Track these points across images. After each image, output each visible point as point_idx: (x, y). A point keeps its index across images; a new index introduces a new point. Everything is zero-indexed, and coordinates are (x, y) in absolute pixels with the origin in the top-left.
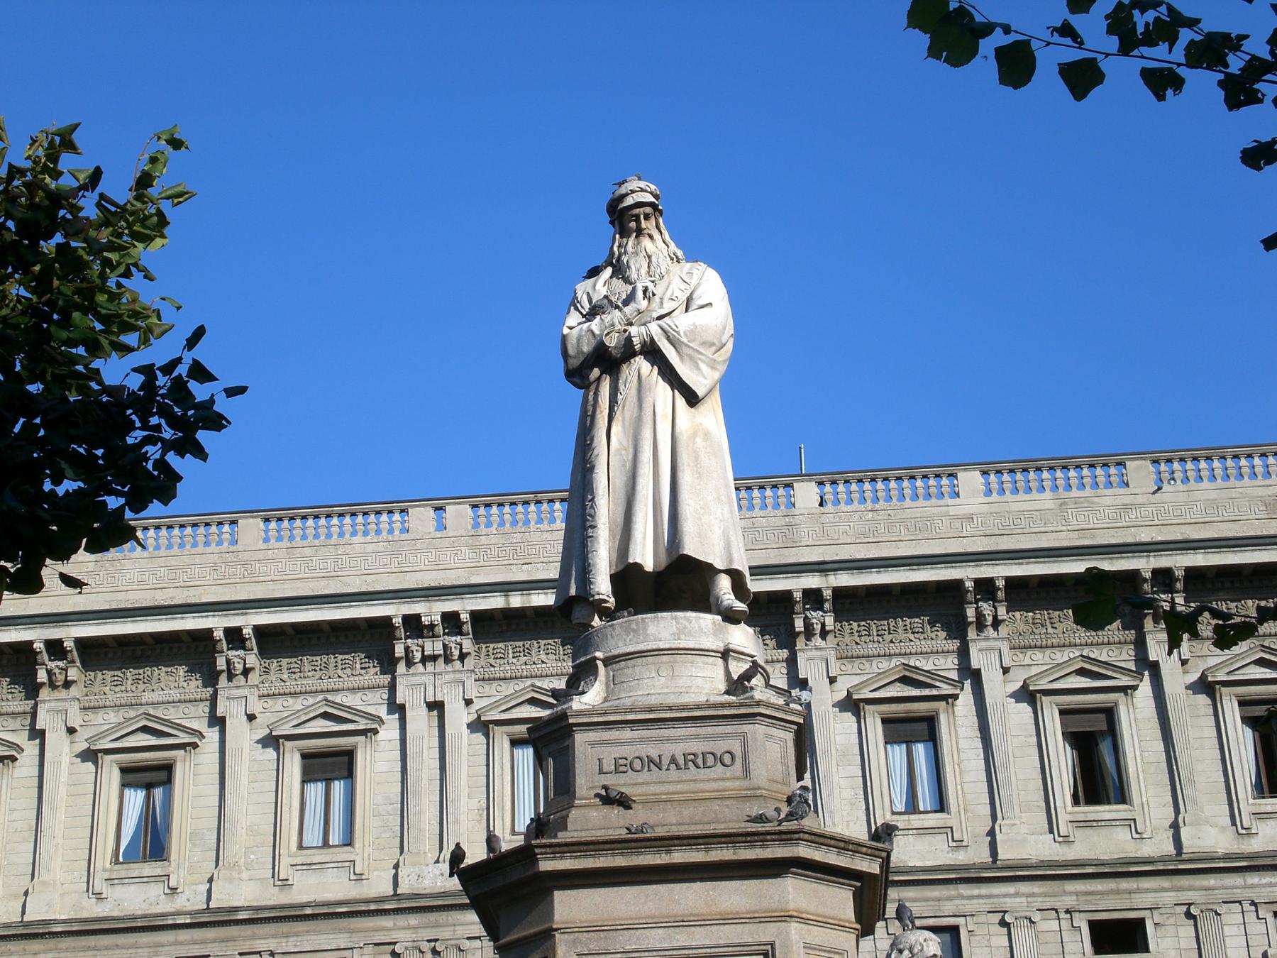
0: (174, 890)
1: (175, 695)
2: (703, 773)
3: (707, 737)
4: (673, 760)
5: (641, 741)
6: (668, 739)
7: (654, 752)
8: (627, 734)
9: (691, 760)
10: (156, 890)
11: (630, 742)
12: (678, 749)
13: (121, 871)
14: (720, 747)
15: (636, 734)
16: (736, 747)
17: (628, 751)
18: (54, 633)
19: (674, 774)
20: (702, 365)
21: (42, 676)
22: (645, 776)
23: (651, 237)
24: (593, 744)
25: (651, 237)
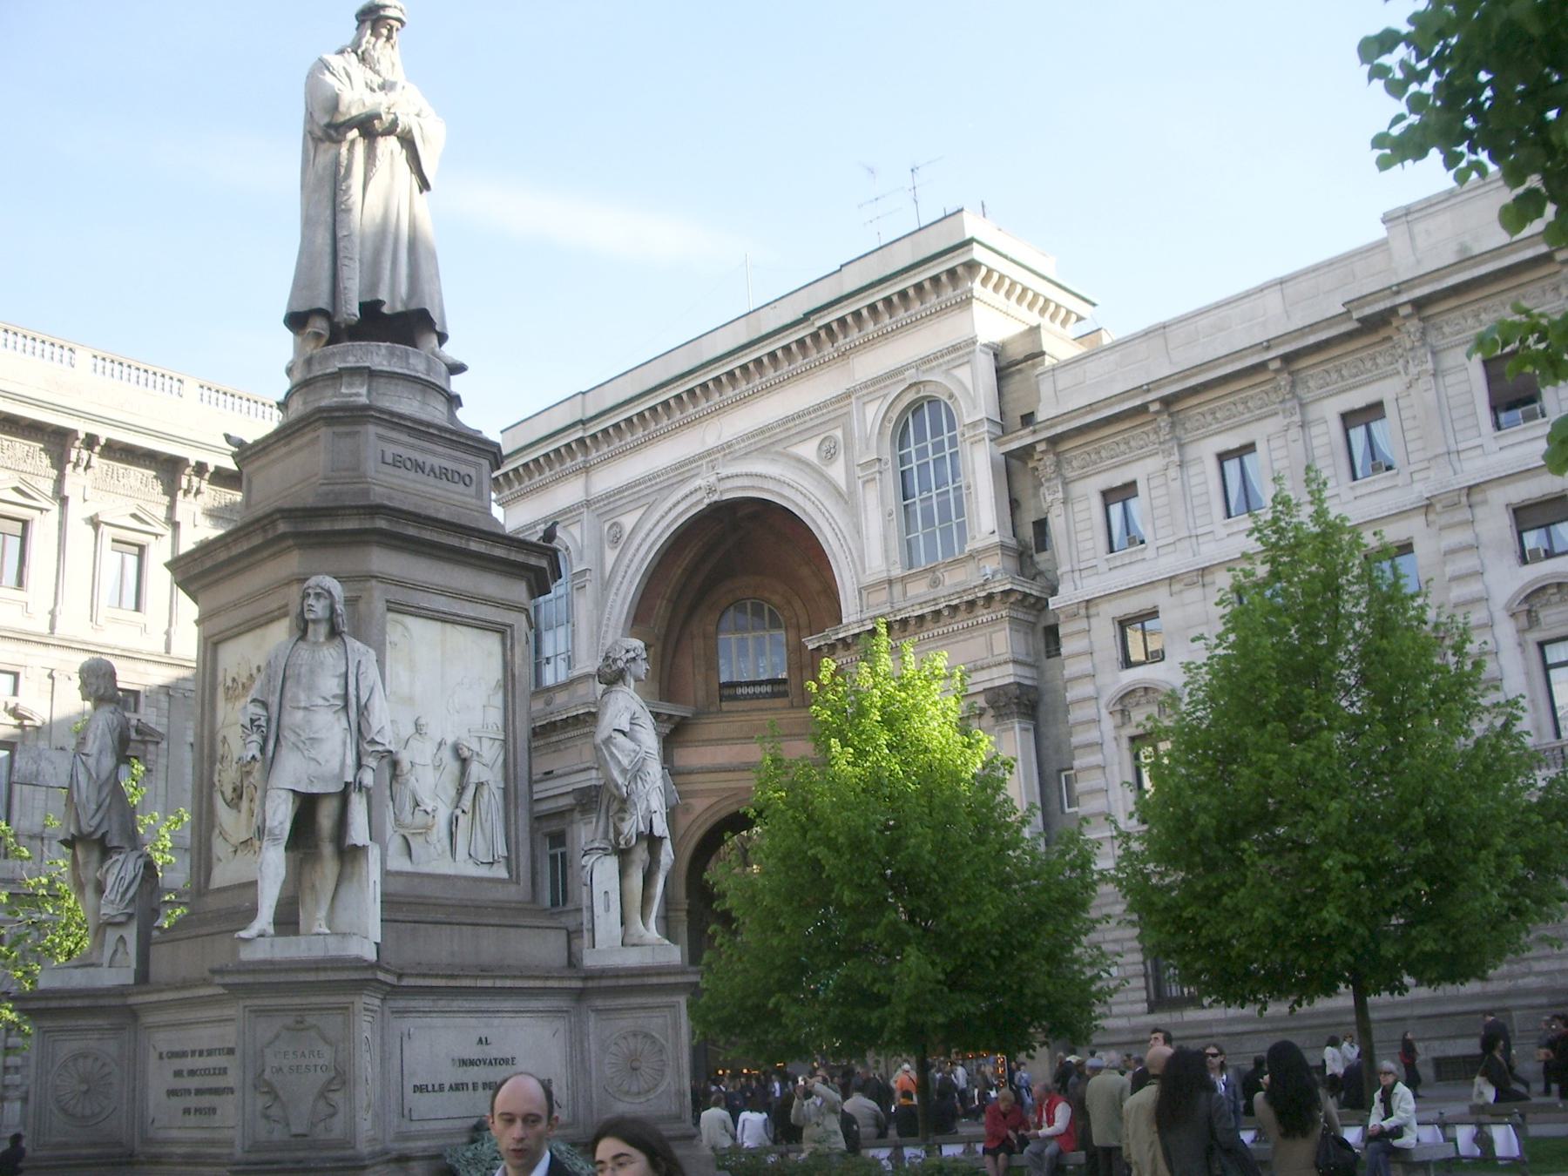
2: (451, 486)
3: (456, 459)
4: (432, 470)
5: (412, 447)
6: (434, 453)
7: (420, 457)
8: (404, 438)
9: (444, 474)
12: (437, 462)
14: (464, 469)
15: (412, 440)
16: (473, 472)
17: (400, 450)
19: (432, 480)
22: (412, 475)
24: (380, 437)
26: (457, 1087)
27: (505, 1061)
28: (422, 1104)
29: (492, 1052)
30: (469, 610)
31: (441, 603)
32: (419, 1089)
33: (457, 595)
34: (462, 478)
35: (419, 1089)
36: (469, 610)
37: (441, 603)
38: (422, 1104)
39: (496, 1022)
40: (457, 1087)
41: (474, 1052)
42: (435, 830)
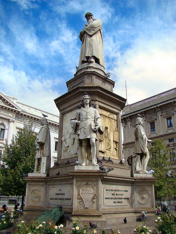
0: (174, 130)
1: (170, 110)
3: (81, 79)
5: (74, 83)
7: (75, 84)
10: (172, 130)
11: (74, 84)
12: (78, 83)
13: (168, 129)
14: (81, 81)
17: (73, 85)
18: (157, 106)
20: (92, 31)
21: (157, 110)
23: (90, 19)
25: (90, 19)
26: (56, 199)
27: (63, 194)
28: (51, 202)
29: (61, 192)
30: (73, 107)
31: (69, 109)
32: (51, 199)
33: (70, 106)
34: (82, 82)
35: (51, 199)
36: (73, 107)
37: (69, 109)
38: (51, 201)
39: (63, 186)
40: (56, 199)
41: (59, 192)
42: (68, 150)
